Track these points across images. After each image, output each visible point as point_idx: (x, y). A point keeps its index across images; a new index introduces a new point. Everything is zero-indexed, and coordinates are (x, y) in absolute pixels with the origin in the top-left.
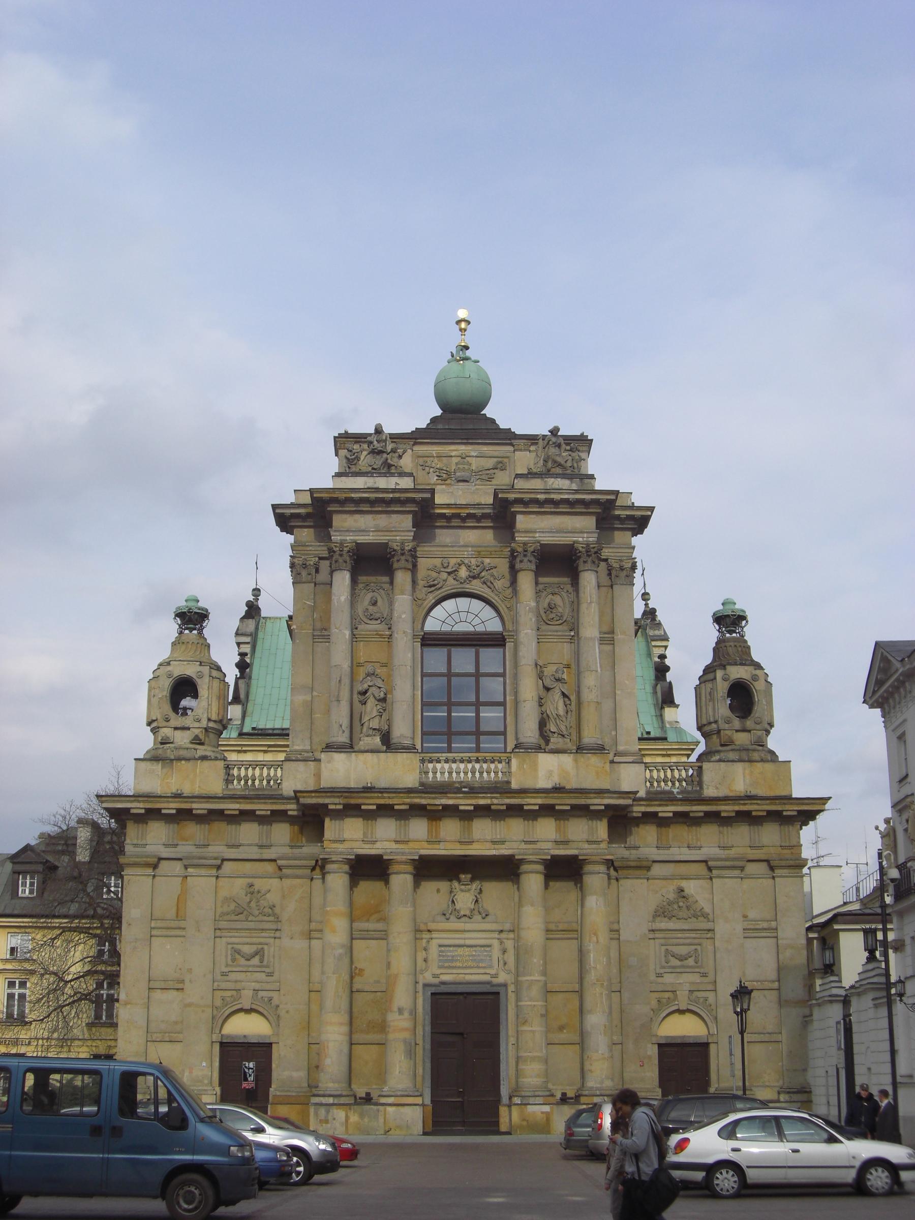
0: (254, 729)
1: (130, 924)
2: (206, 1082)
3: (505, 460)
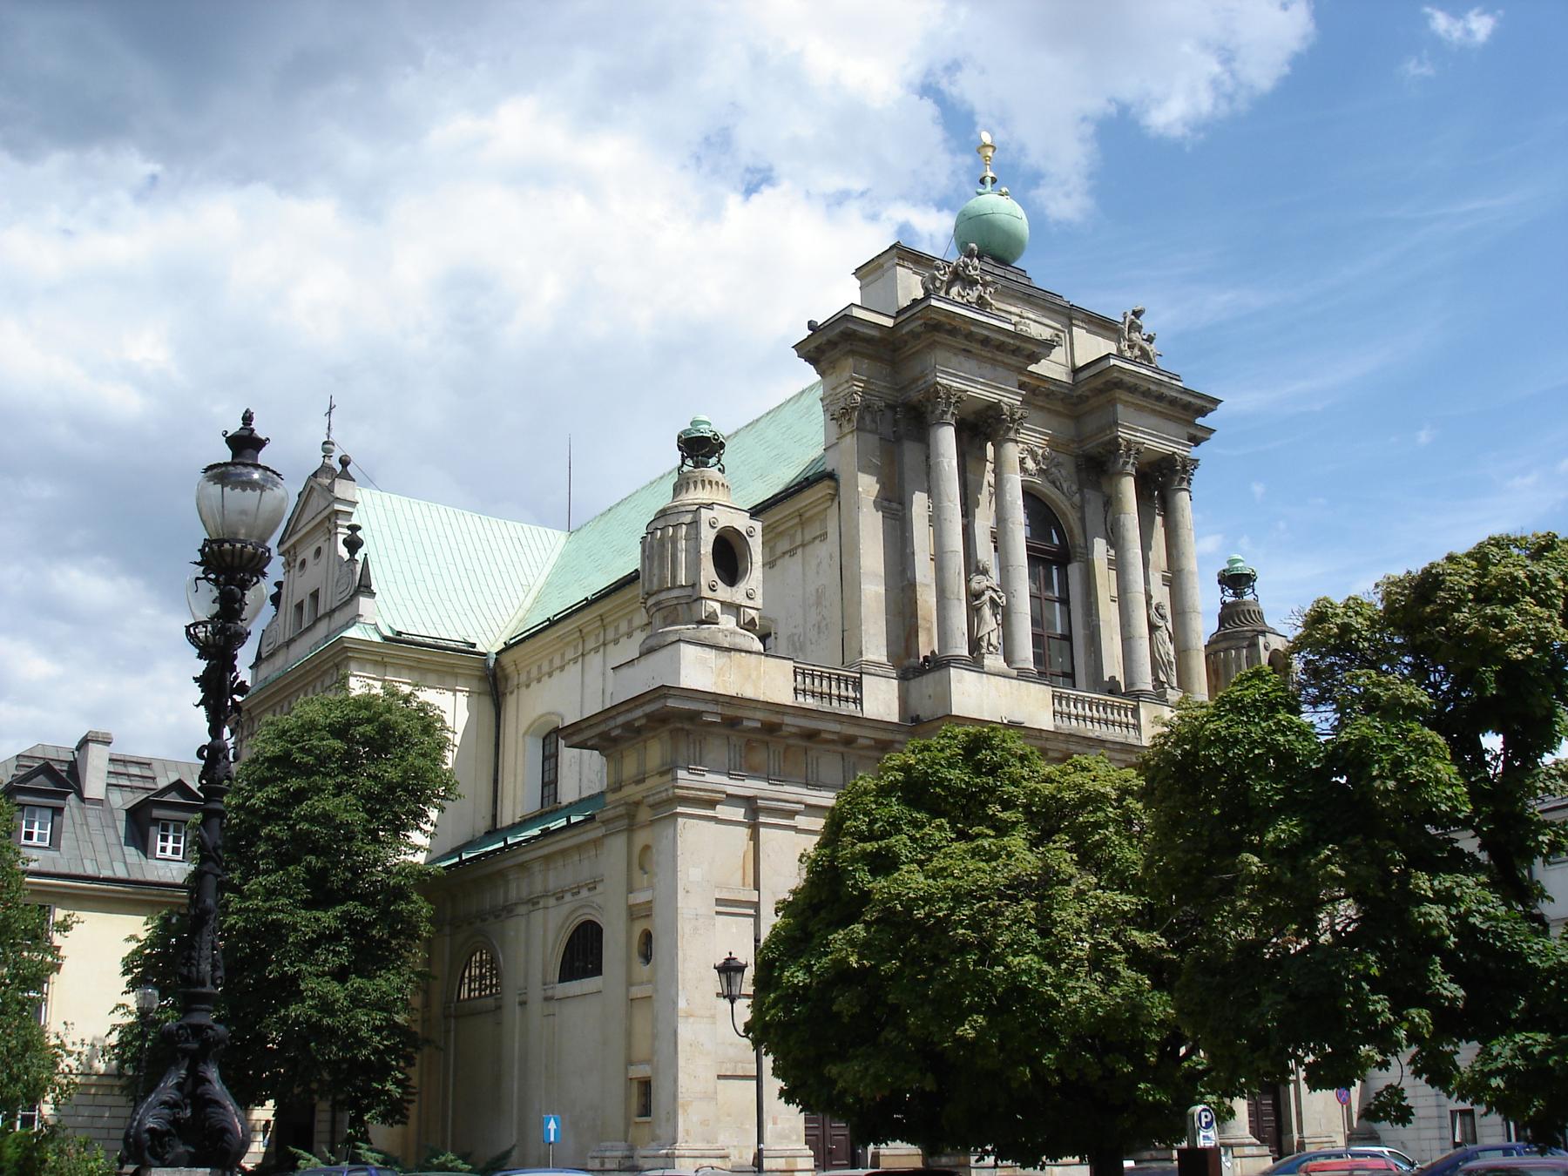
0: (399, 633)
1: (687, 892)
2: (794, 1138)
3: (1061, 334)
